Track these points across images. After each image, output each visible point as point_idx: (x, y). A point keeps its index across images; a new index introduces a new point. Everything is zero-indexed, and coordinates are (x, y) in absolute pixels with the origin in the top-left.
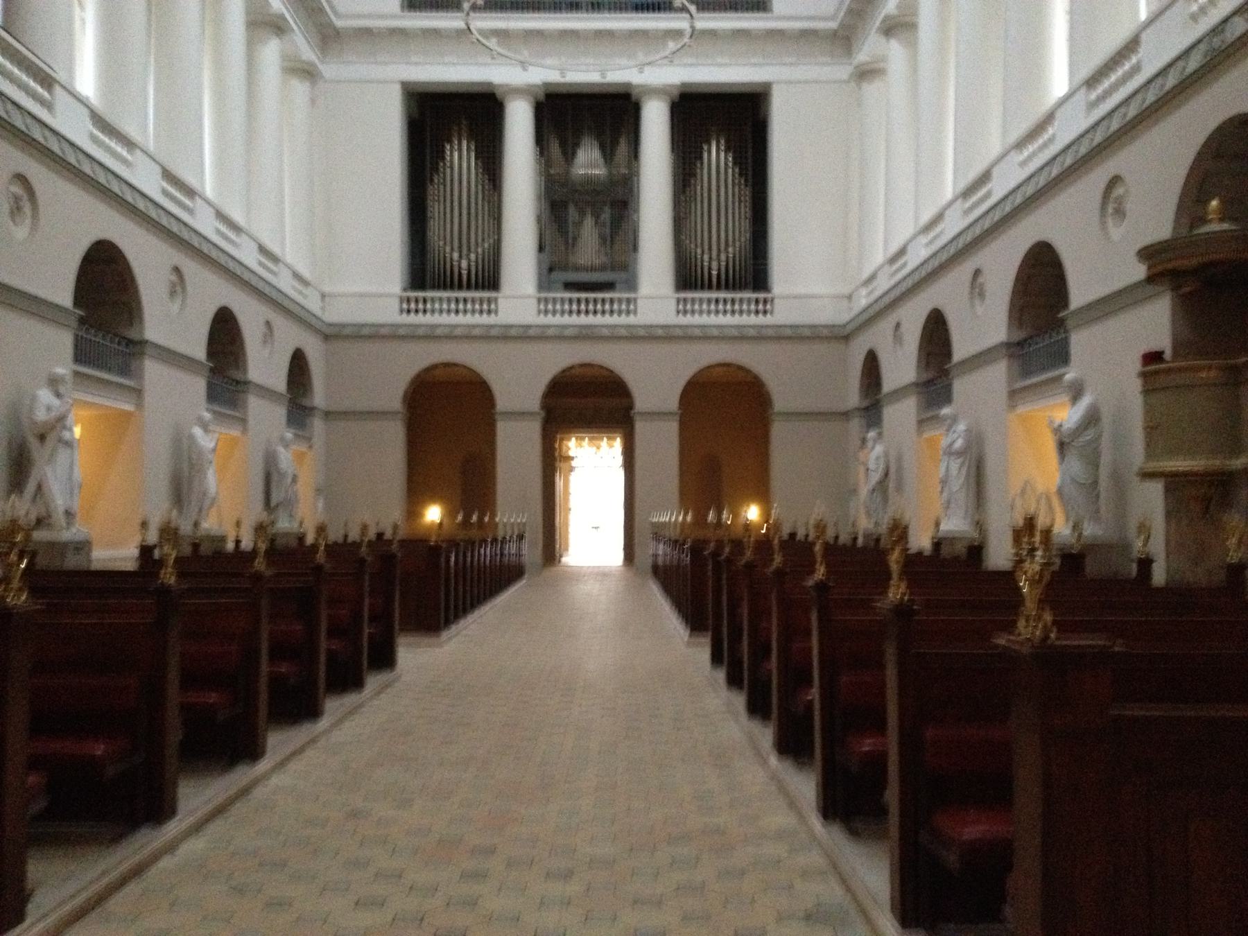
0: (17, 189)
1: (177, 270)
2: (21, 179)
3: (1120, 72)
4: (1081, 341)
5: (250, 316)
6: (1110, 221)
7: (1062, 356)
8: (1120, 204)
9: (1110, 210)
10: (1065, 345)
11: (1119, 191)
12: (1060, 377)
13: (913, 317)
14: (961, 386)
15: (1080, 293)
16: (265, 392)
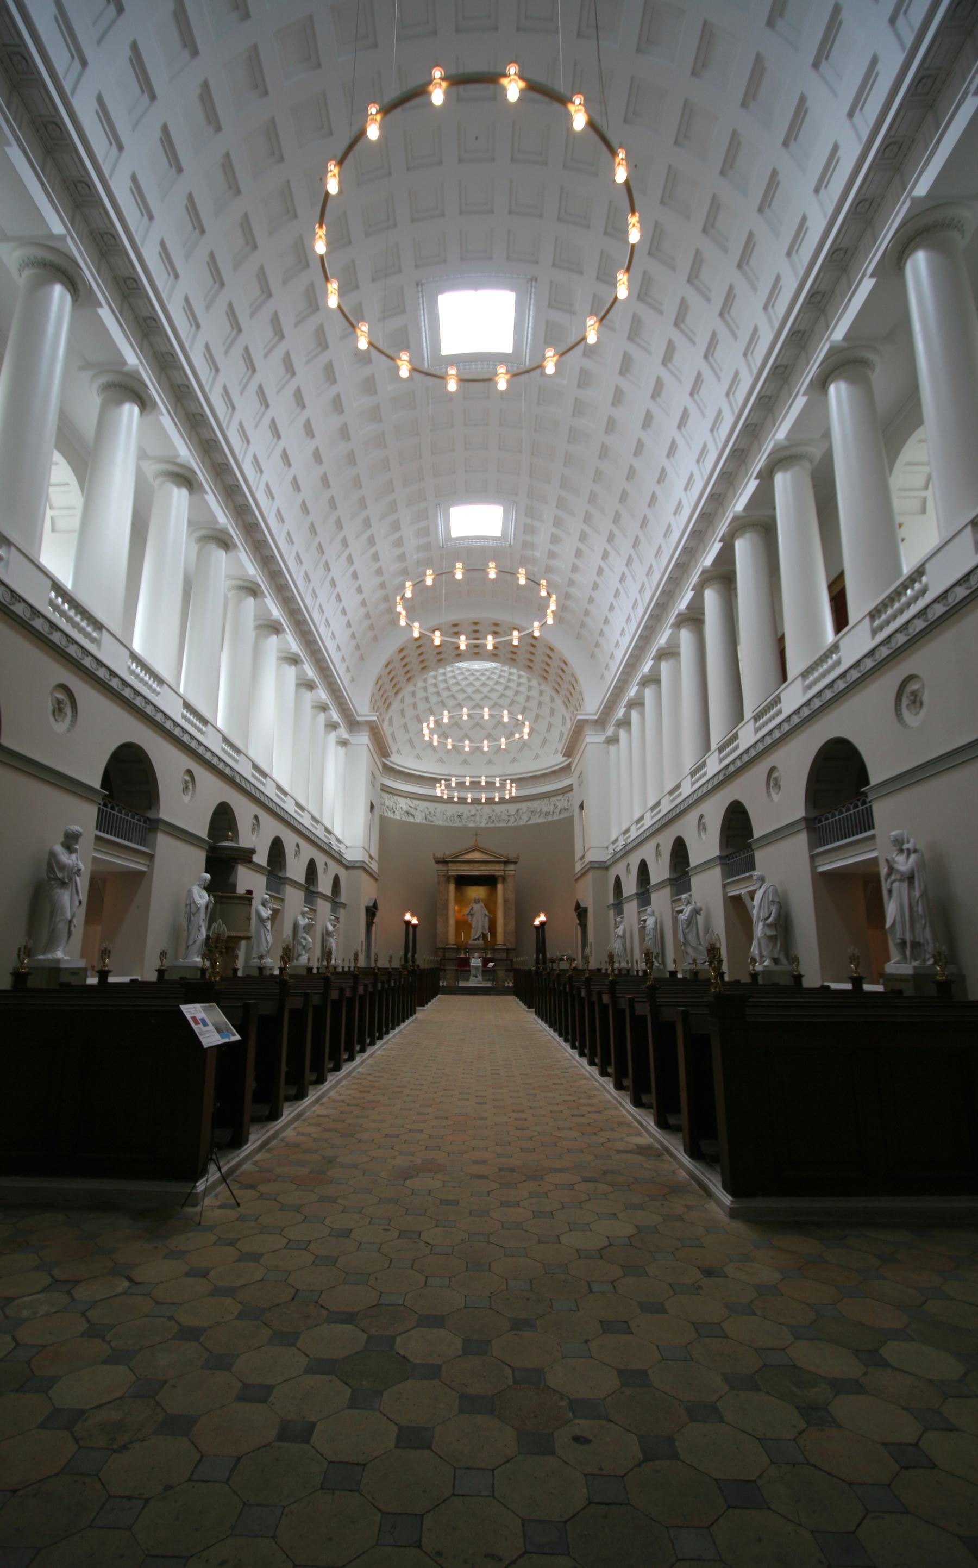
0: (187, 778)
1: (256, 817)
2: (189, 772)
3: (768, 715)
4: (761, 857)
5: (290, 840)
6: (772, 792)
7: (750, 865)
8: (777, 782)
9: (772, 784)
10: (752, 858)
11: (775, 774)
12: (751, 877)
13: (666, 841)
14: (695, 881)
15: (758, 831)
16: (295, 884)
